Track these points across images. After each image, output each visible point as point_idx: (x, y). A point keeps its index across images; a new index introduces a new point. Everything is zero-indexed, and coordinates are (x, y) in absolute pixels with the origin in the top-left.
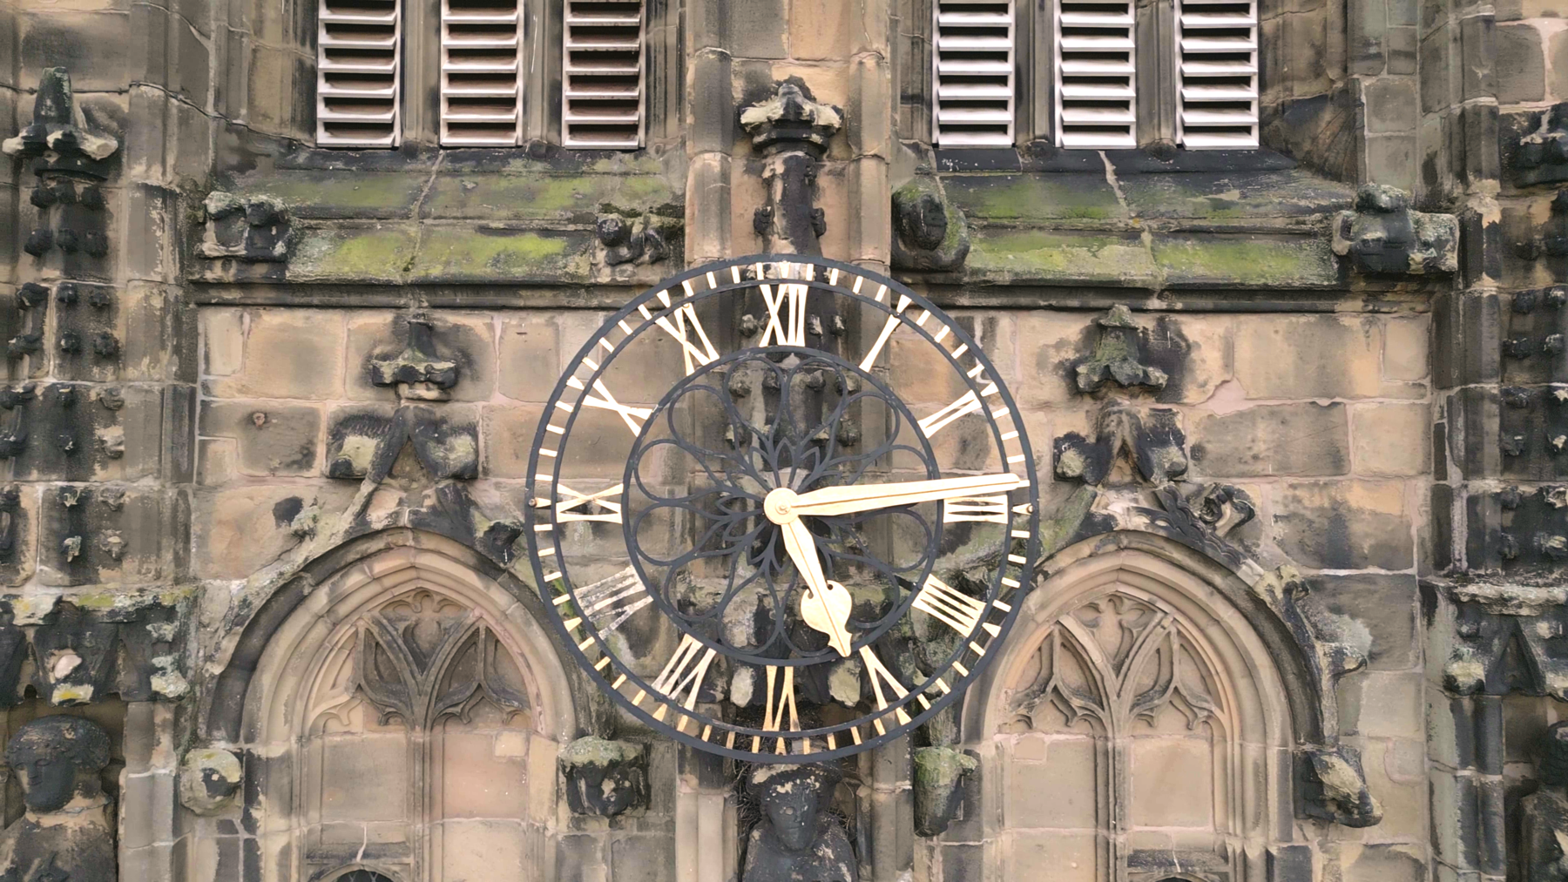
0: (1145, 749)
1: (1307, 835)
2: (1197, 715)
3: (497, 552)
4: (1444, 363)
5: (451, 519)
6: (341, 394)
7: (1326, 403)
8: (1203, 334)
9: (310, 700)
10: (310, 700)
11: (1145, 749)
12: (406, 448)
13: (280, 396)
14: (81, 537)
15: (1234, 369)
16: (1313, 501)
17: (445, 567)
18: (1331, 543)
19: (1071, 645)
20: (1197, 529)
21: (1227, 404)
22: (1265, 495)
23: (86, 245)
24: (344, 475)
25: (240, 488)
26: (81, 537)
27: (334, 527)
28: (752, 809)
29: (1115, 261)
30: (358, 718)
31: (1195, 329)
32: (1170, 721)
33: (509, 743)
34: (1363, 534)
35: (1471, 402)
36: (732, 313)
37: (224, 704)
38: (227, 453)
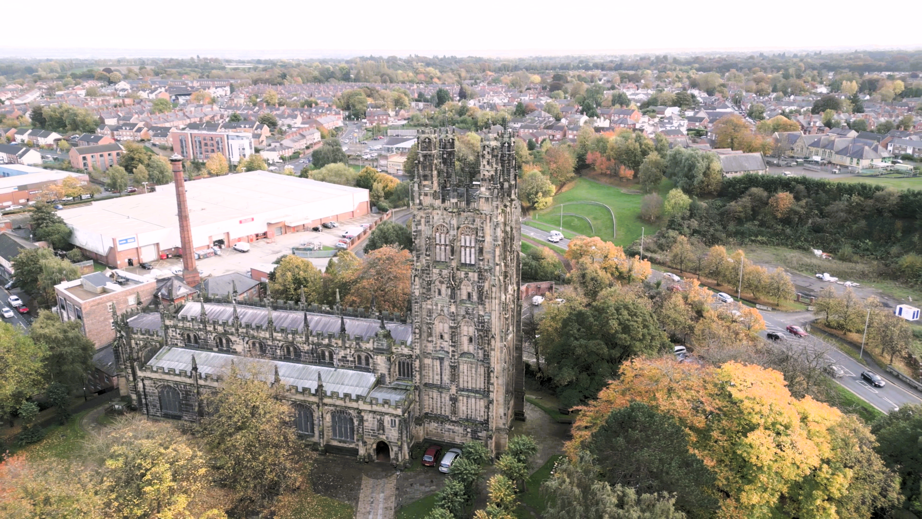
9: (437, 283)
10: (437, 283)
15: (471, 274)
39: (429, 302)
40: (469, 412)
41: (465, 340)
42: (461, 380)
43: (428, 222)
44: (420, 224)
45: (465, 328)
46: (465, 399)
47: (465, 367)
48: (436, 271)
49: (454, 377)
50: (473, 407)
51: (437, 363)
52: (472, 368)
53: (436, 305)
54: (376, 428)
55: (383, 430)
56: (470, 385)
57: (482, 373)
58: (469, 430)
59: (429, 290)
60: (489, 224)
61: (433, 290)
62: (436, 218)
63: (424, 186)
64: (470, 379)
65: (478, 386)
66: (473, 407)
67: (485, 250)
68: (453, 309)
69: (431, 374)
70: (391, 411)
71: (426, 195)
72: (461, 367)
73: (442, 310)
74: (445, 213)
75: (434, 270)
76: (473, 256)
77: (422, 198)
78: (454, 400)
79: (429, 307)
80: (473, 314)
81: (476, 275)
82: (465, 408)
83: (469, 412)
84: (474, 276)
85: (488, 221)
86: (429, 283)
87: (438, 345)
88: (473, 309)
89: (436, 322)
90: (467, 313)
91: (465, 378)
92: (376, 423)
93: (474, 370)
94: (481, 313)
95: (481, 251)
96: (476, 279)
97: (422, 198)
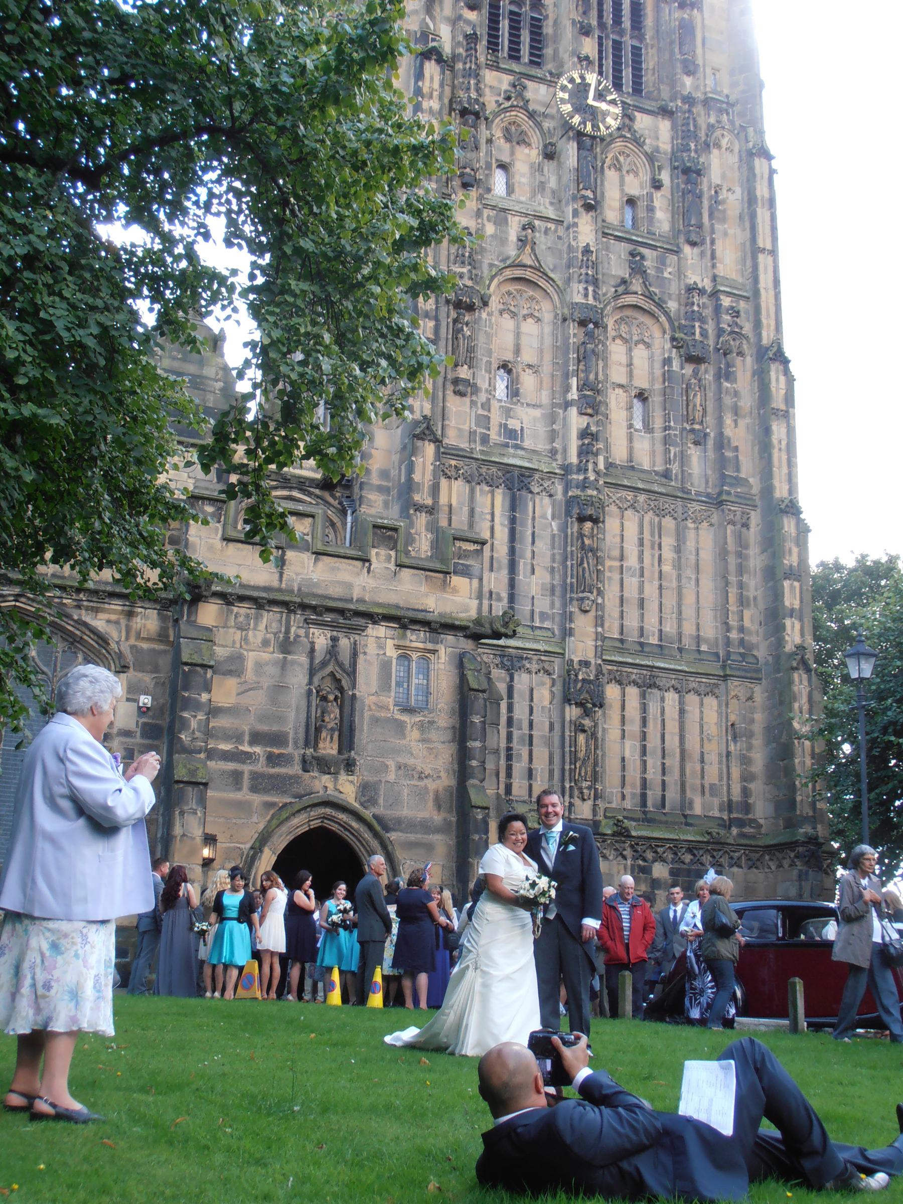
1: (653, 190)
2: (636, 174)
3: (532, 115)
4: (674, 127)
11: (629, 178)
13: (495, 84)
15: (642, 122)
16: (654, 143)
17: (522, 117)
18: (657, 150)
19: (617, 160)
20: (638, 142)
21: (642, 126)
30: (502, 141)
31: (636, 114)
32: (631, 175)
33: (527, 151)
34: (662, 150)
35: (677, 132)
40: (654, 774)
42: (611, 593)
46: (633, 692)
48: (497, 83)
49: (581, 577)
50: (673, 742)
51: (493, 503)
54: (292, 722)
55: (347, 737)
56: (651, 622)
57: (707, 556)
58: (660, 871)
64: (651, 590)
65: (689, 629)
66: (673, 742)
70: (413, 592)
72: (612, 524)
75: (490, 77)
78: (582, 694)
82: (631, 749)
83: (654, 774)
87: (496, 417)
89: (494, 304)
91: (631, 583)
92: (298, 679)
93: (668, 542)
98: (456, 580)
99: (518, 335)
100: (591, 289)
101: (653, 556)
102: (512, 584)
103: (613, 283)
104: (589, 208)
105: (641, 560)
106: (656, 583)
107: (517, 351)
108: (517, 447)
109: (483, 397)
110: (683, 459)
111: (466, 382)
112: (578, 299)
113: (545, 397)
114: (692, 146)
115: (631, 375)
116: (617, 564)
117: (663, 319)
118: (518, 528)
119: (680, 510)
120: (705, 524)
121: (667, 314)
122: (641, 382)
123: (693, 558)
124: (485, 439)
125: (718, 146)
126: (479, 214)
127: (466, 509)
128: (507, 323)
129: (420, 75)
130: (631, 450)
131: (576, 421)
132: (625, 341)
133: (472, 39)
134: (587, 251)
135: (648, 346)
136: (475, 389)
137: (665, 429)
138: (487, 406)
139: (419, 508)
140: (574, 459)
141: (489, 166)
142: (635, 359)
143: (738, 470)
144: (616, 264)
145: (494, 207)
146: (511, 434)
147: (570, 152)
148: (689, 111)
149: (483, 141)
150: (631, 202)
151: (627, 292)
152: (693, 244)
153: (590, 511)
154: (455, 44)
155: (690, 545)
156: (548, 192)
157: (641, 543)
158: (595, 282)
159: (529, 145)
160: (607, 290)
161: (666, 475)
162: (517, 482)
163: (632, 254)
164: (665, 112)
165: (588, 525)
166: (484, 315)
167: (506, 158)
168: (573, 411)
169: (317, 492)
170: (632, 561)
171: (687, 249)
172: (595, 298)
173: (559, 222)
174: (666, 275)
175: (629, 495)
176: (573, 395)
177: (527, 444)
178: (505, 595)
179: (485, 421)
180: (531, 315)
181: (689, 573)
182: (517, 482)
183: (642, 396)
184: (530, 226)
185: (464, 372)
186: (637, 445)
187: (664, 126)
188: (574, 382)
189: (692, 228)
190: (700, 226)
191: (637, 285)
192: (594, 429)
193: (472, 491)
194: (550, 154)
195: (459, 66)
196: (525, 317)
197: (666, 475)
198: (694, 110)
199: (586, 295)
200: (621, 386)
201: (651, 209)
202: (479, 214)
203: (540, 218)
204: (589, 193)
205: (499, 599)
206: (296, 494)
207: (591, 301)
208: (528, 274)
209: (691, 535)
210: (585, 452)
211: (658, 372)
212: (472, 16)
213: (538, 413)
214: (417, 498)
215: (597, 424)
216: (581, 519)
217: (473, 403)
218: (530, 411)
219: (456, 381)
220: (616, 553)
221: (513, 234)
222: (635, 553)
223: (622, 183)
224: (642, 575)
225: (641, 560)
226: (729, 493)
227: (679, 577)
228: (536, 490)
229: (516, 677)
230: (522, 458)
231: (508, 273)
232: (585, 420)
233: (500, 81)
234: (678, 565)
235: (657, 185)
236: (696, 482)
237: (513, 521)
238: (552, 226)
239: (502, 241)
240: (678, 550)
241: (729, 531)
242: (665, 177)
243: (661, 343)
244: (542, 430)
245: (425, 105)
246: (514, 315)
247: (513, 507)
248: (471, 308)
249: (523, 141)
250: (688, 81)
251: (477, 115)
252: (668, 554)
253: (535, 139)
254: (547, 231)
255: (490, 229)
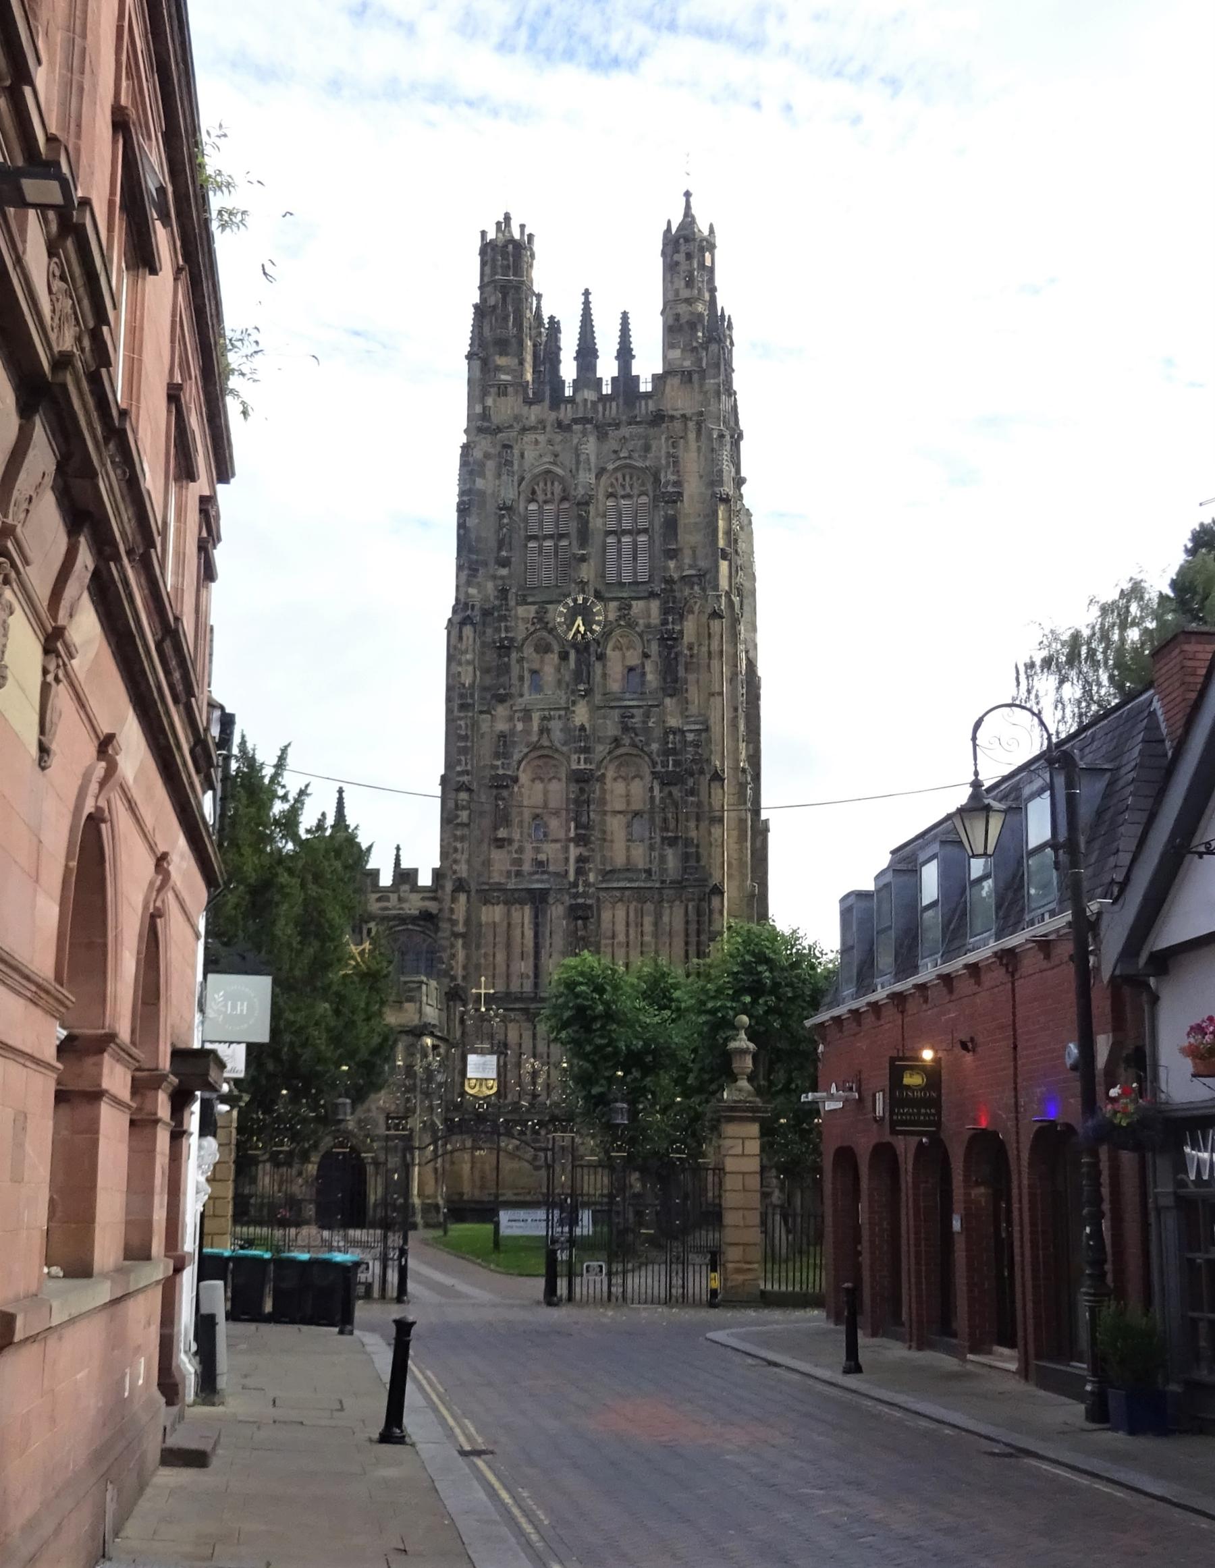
0: (628, 654)
5: (545, 628)
6: (532, 615)
7: (648, 610)
8: (634, 603)
10: (529, 651)
11: (628, 654)
12: (540, 620)
13: (525, 615)
14: (507, 629)
15: (638, 606)
17: (545, 634)
18: (648, 626)
20: (631, 625)
22: (641, 622)
23: (506, 599)
24: (533, 624)
25: (522, 626)
26: (507, 629)
27: (532, 629)
28: (578, 651)
29: (625, 595)
36: (575, 600)
37: (520, 649)
38: (520, 623)
39: (501, 711)
41: (616, 825)
43: (509, 463)
44: (482, 475)
45: (620, 788)
47: (620, 913)
48: (526, 612)
51: (524, 915)
52: (641, 914)
53: (527, 715)
59: (505, 669)
60: (693, 445)
61: (515, 670)
62: (530, 455)
63: (498, 369)
67: (682, 522)
68: (581, 714)
69: (500, 958)
71: (502, 390)
72: (606, 916)
73: (544, 730)
74: (559, 438)
75: (521, 611)
76: (643, 558)
77: (489, 402)
79: (502, 726)
80: (647, 730)
81: (655, 605)
84: (648, 611)
85: (692, 436)
86: (504, 648)
87: (528, 855)
88: (647, 716)
89: (524, 778)
90: (626, 729)
93: (648, 921)
94: (673, 722)
95: (671, 525)
96: (655, 619)
97: (489, 402)
98: (407, 1005)
99: (546, 793)
100: (582, 757)
101: (636, 932)
102: (536, 967)
103: (608, 741)
104: (583, 697)
105: (627, 935)
106: (639, 949)
107: (545, 806)
108: (543, 873)
109: (516, 845)
110: (663, 859)
111: (503, 840)
112: (574, 766)
113: (562, 835)
114: (670, 619)
115: (628, 803)
116: (610, 941)
117: (647, 758)
118: (541, 929)
119: (656, 897)
120: (677, 903)
121: (650, 755)
122: (637, 806)
123: (668, 928)
124: (518, 874)
125: (693, 612)
126: (511, 719)
127: (505, 924)
128: (539, 786)
129: (461, 638)
130: (628, 858)
131: (574, 852)
132: (624, 779)
133: (503, 593)
134: (583, 728)
135: (642, 778)
136: (510, 841)
137: (651, 838)
138: (520, 850)
139: (463, 936)
140: (572, 878)
141: (521, 678)
142: (625, 791)
143: (698, 861)
144: (611, 728)
145: (521, 711)
146: (540, 864)
147: (573, 655)
148: (672, 591)
149: (513, 662)
150: (631, 669)
151: (618, 746)
152: (671, 696)
153: (580, 913)
154: (497, 597)
155: (666, 919)
156: (564, 685)
157: (628, 925)
158: (586, 750)
159: (552, 652)
160: (601, 750)
161: (649, 872)
162: (538, 899)
163: (623, 717)
164: (652, 595)
165: (580, 922)
166: (516, 789)
167: (536, 666)
168: (572, 845)
169: (422, 923)
170: (621, 938)
171: (668, 701)
172: (585, 763)
173: (567, 709)
174: (650, 724)
175: (618, 894)
176: (572, 834)
177: (551, 868)
178: (531, 974)
179: (518, 862)
180: (554, 778)
181: (666, 939)
182: (538, 899)
183: (636, 814)
184: (544, 718)
185: (502, 833)
186: (634, 852)
187: (655, 605)
188: (572, 825)
189: (672, 685)
190: (676, 681)
191: (627, 741)
192: (586, 854)
193: (509, 911)
194: (564, 657)
195: (496, 614)
196: (550, 780)
197: (649, 872)
198: (675, 587)
199: (579, 762)
200: (620, 812)
201: (644, 674)
202: (511, 719)
203: (555, 709)
204: (581, 687)
205: (528, 977)
206: (410, 927)
207: (582, 766)
208: (545, 752)
209: (667, 912)
210: (579, 872)
211: (647, 798)
212: (504, 572)
213: (558, 846)
214: (455, 929)
215: (588, 850)
216: (577, 918)
217: (509, 852)
218: (553, 845)
219: (497, 840)
220: (609, 934)
221: (535, 728)
222: (624, 932)
223: (624, 657)
224: (628, 946)
225: (627, 935)
226: (687, 880)
227: (656, 944)
228: (551, 901)
229: (538, 1027)
230: (542, 881)
231: (533, 755)
232: (580, 850)
233: (529, 612)
234: (656, 935)
235: (646, 656)
236: (671, 872)
237: (536, 925)
238: (562, 713)
239: (527, 732)
240: (656, 924)
241: (690, 907)
242: (654, 648)
243: (648, 777)
244: (561, 856)
245: (463, 658)
246: (542, 780)
247: (536, 917)
248: (507, 787)
249: (547, 649)
250: (672, 564)
251: (508, 648)
252: (648, 927)
253: (556, 648)
254: (560, 717)
255: (520, 726)
